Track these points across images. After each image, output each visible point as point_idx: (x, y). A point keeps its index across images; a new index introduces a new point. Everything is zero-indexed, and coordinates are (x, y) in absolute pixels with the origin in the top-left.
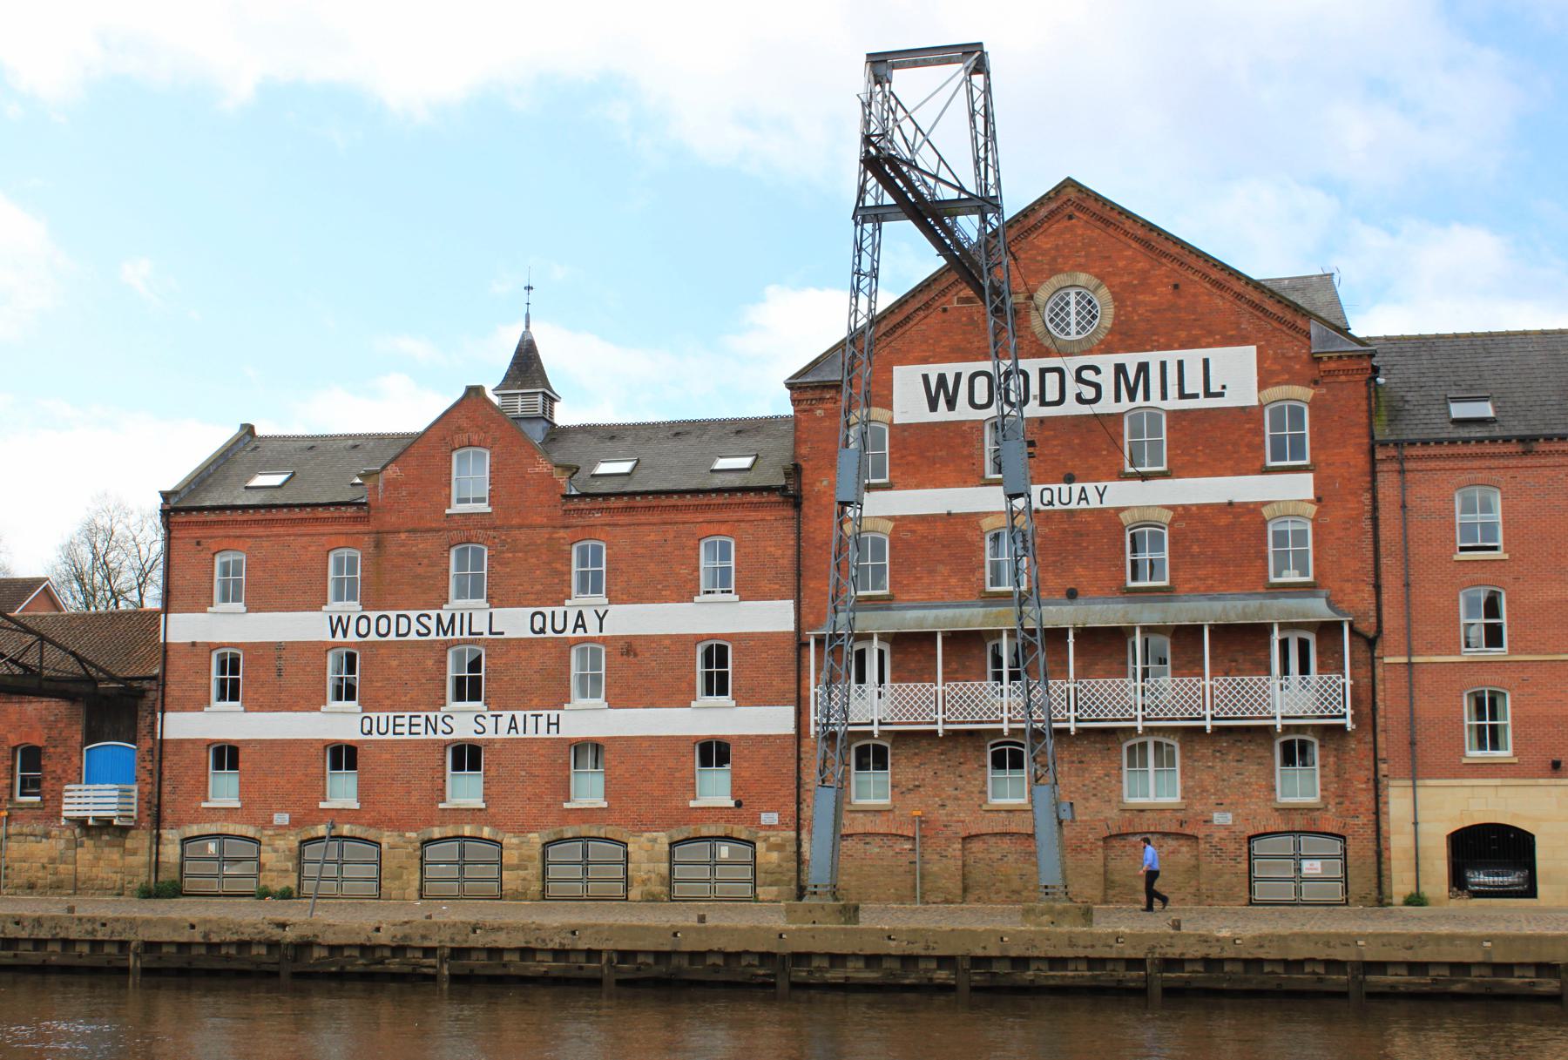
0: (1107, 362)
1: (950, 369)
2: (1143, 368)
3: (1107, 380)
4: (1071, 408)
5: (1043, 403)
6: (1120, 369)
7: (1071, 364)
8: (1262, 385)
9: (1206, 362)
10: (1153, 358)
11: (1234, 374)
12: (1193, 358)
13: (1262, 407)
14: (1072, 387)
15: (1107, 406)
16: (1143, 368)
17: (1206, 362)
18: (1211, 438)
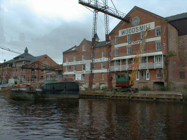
0: (139, 26)
1: (124, 30)
2: (143, 26)
3: (139, 28)
4: (135, 32)
5: (133, 32)
6: (140, 27)
7: (135, 27)
8: (155, 26)
9: (149, 24)
10: (143, 25)
11: (152, 26)
12: (148, 24)
13: (155, 29)
14: (136, 30)
15: (139, 31)
16: (143, 26)
17: (149, 24)
18: (151, 33)
